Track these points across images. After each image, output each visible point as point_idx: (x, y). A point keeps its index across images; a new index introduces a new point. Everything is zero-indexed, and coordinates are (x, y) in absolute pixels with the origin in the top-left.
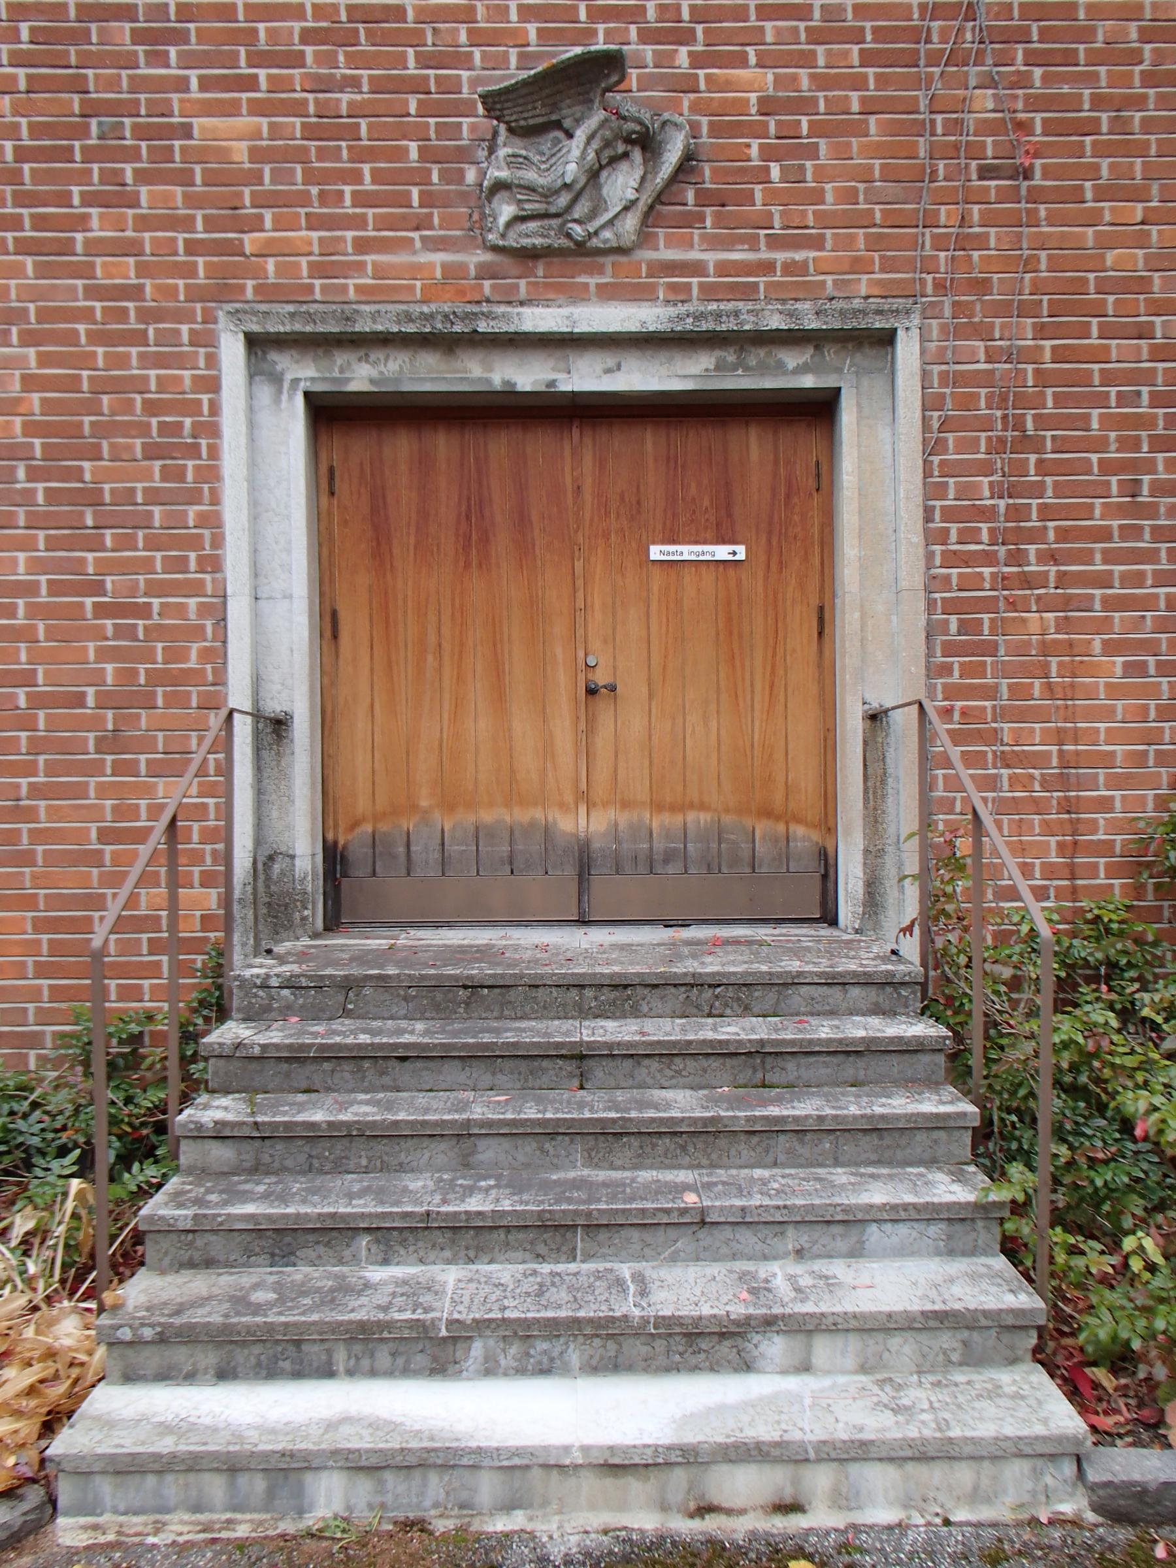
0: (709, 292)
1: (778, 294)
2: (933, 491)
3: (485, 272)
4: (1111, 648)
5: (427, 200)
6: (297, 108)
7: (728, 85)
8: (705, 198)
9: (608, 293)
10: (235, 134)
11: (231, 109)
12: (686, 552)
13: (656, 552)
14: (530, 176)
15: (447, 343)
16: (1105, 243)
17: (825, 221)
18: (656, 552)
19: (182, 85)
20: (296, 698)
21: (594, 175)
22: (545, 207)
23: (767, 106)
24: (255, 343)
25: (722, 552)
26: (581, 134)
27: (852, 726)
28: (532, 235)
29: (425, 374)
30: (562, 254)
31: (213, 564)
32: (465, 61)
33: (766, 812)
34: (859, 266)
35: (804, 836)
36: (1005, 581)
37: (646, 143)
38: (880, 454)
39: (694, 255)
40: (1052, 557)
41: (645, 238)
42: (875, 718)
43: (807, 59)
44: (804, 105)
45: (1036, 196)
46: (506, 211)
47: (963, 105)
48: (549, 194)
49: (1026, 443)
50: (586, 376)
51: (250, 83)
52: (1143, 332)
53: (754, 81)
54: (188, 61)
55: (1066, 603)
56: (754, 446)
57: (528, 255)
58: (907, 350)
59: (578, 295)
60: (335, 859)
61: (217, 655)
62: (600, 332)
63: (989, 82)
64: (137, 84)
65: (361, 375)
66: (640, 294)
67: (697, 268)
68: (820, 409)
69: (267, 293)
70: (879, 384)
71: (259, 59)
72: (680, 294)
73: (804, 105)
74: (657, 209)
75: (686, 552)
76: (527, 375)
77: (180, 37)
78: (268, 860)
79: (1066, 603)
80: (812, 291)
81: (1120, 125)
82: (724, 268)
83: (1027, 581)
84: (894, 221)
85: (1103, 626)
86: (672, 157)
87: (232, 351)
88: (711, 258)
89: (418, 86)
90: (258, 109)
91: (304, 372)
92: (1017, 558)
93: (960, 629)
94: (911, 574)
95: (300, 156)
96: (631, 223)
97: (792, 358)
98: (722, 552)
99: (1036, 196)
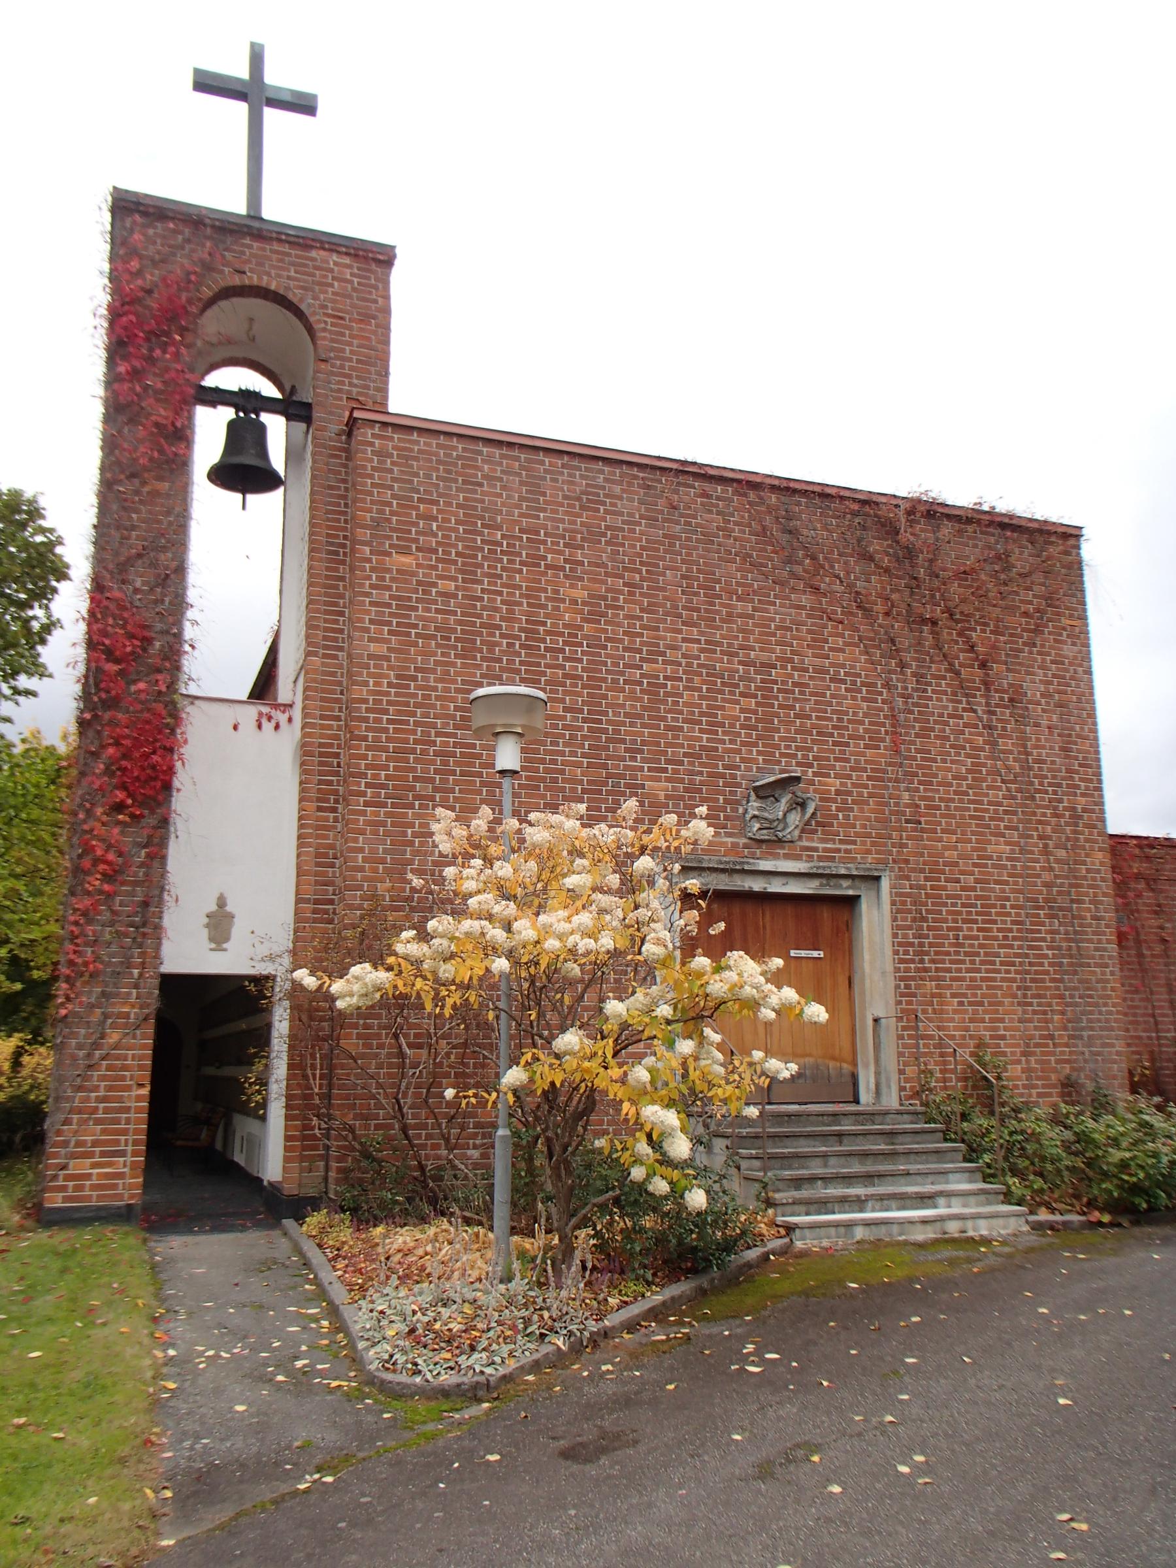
0: (820, 859)
1: (843, 860)
2: (895, 936)
3: (746, 846)
4: (953, 996)
5: (726, 818)
6: (682, 781)
7: (825, 784)
8: (818, 824)
9: (787, 857)
11: (659, 780)
12: (803, 953)
14: (766, 815)
15: (731, 872)
16: (945, 848)
17: (857, 835)
18: (793, 953)
19: (641, 769)
22: (769, 825)
23: (838, 793)
25: (815, 954)
26: (784, 801)
27: (870, 1023)
28: (764, 835)
30: (774, 844)
32: (738, 768)
33: (834, 1058)
34: (868, 852)
35: (846, 1067)
36: (918, 970)
37: (803, 805)
38: (875, 922)
39: (814, 845)
40: (933, 961)
41: (800, 838)
42: (876, 1020)
43: (849, 777)
44: (849, 793)
45: (923, 830)
46: (757, 826)
47: (899, 797)
48: (772, 821)
49: (925, 920)
50: (776, 887)
51: (665, 770)
52: (958, 881)
53: (834, 784)
54: (644, 760)
55: (938, 979)
56: (825, 913)
58: (885, 884)
59: (776, 857)
62: (784, 872)
63: (907, 790)
64: (626, 768)
66: (797, 858)
67: (816, 849)
68: (851, 902)
70: (873, 893)
71: (668, 762)
73: (849, 793)
75: (803, 953)
76: (757, 885)
77: (641, 752)
79: (938, 979)
81: (948, 808)
82: (825, 850)
83: (926, 970)
84: (879, 836)
85: (950, 987)
86: (810, 810)
88: (821, 846)
89: (723, 776)
90: (668, 780)
92: (922, 961)
94: (889, 968)
95: (682, 798)
96: (797, 833)
97: (845, 883)
98: (815, 954)
99: (923, 830)
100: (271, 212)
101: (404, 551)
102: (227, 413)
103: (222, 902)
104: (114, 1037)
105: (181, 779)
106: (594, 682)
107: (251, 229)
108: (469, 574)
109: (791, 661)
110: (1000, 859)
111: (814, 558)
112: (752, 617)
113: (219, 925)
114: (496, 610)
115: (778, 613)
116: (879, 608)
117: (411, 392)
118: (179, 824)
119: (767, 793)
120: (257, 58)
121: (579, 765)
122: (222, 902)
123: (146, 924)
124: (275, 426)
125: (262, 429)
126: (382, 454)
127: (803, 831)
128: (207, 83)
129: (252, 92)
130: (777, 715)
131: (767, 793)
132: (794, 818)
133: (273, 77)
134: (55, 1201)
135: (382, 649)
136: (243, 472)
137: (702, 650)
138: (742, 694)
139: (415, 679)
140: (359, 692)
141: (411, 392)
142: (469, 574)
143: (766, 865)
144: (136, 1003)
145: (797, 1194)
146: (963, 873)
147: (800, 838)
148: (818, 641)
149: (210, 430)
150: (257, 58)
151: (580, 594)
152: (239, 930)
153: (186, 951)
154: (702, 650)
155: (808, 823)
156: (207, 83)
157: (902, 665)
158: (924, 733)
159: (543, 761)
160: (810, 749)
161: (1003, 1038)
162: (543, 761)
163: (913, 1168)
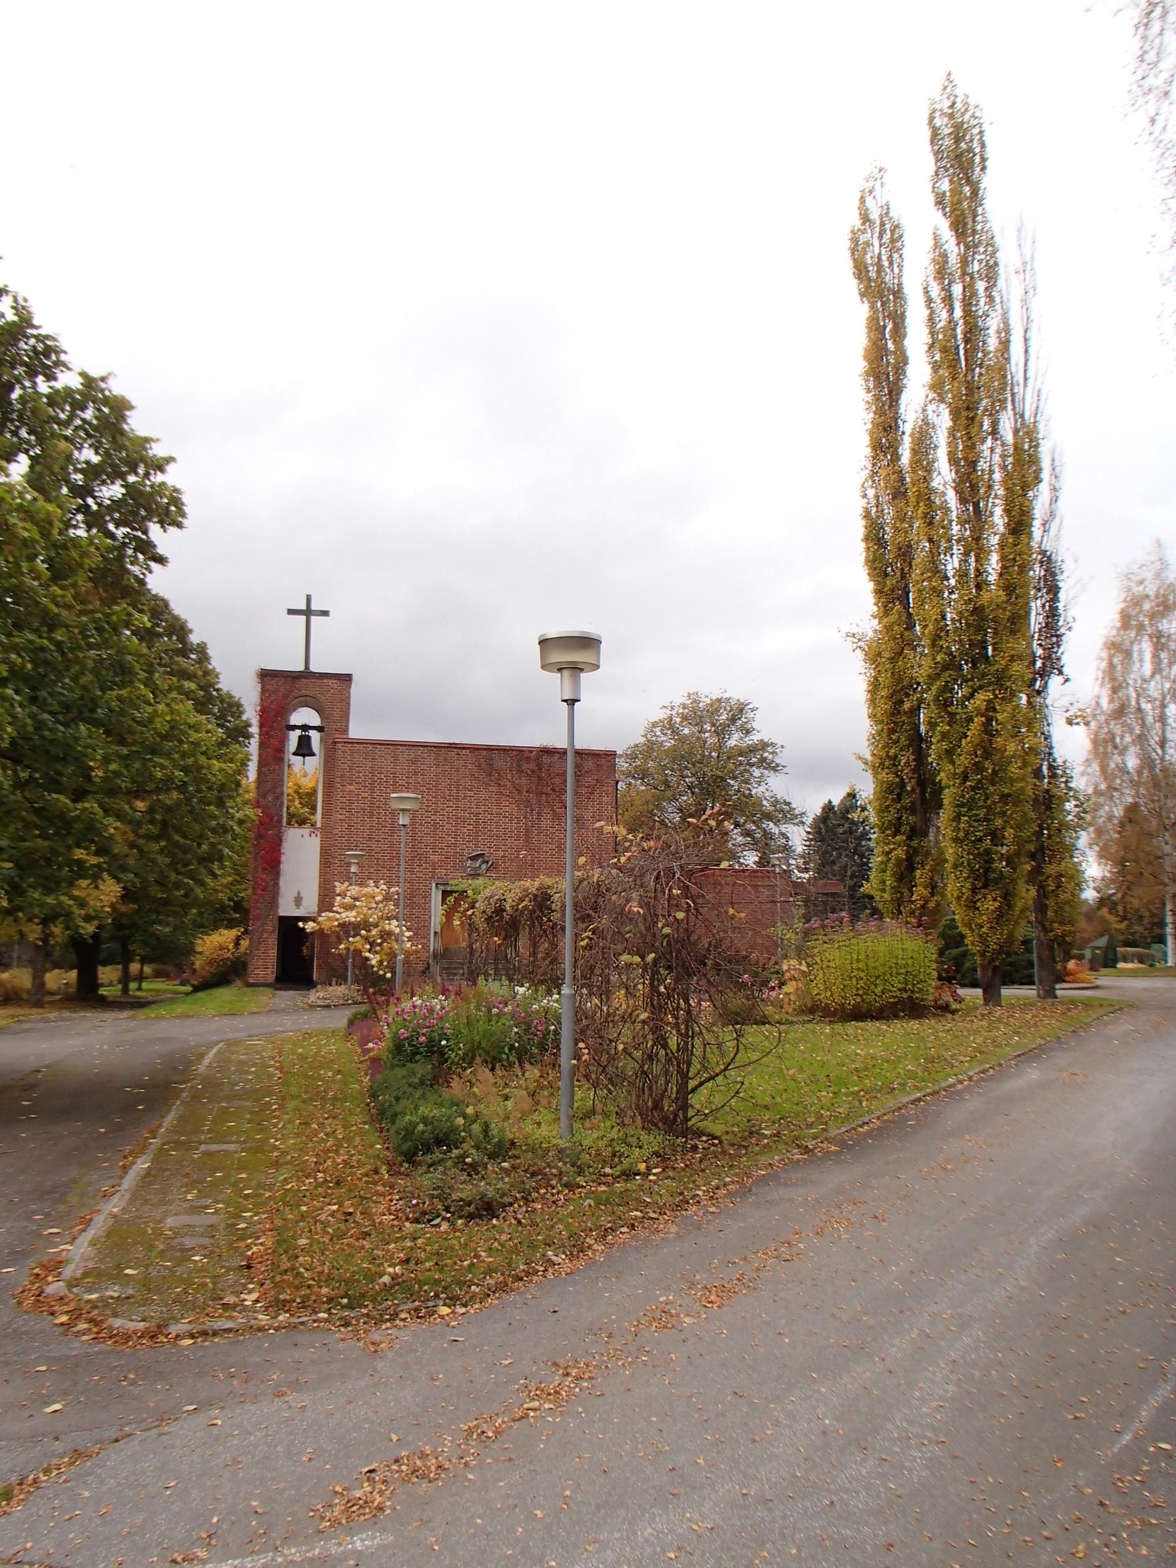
10: (436, 858)
20: (439, 930)
22: (475, 869)
87: (434, 885)
91: (442, 888)
100: (313, 668)
101: (351, 784)
102: (298, 732)
103: (299, 893)
104: (265, 935)
105: (283, 858)
107: (307, 674)
111: (499, 774)
113: (298, 901)
115: (483, 795)
116: (524, 789)
117: (356, 731)
118: (282, 872)
119: (474, 858)
120: (309, 599)
122: (299, 893)
123: (274, 903)
124: (315, 736)
125: (309, 738)
128: (291, 612)
129: (308, 613)
131: (474, 858)
132: (484, 866)
133: (314, 607)
134: (251, 981)
136: (304, 749)
140: (336, 831)
141: (356, 731)
144: (271, 926)
148: (499, 804)
149: (294, 736)
150: (309, 599)
152: (304, 902)
153: (286, 909)
156: (291, 612)
157: (532, 810)
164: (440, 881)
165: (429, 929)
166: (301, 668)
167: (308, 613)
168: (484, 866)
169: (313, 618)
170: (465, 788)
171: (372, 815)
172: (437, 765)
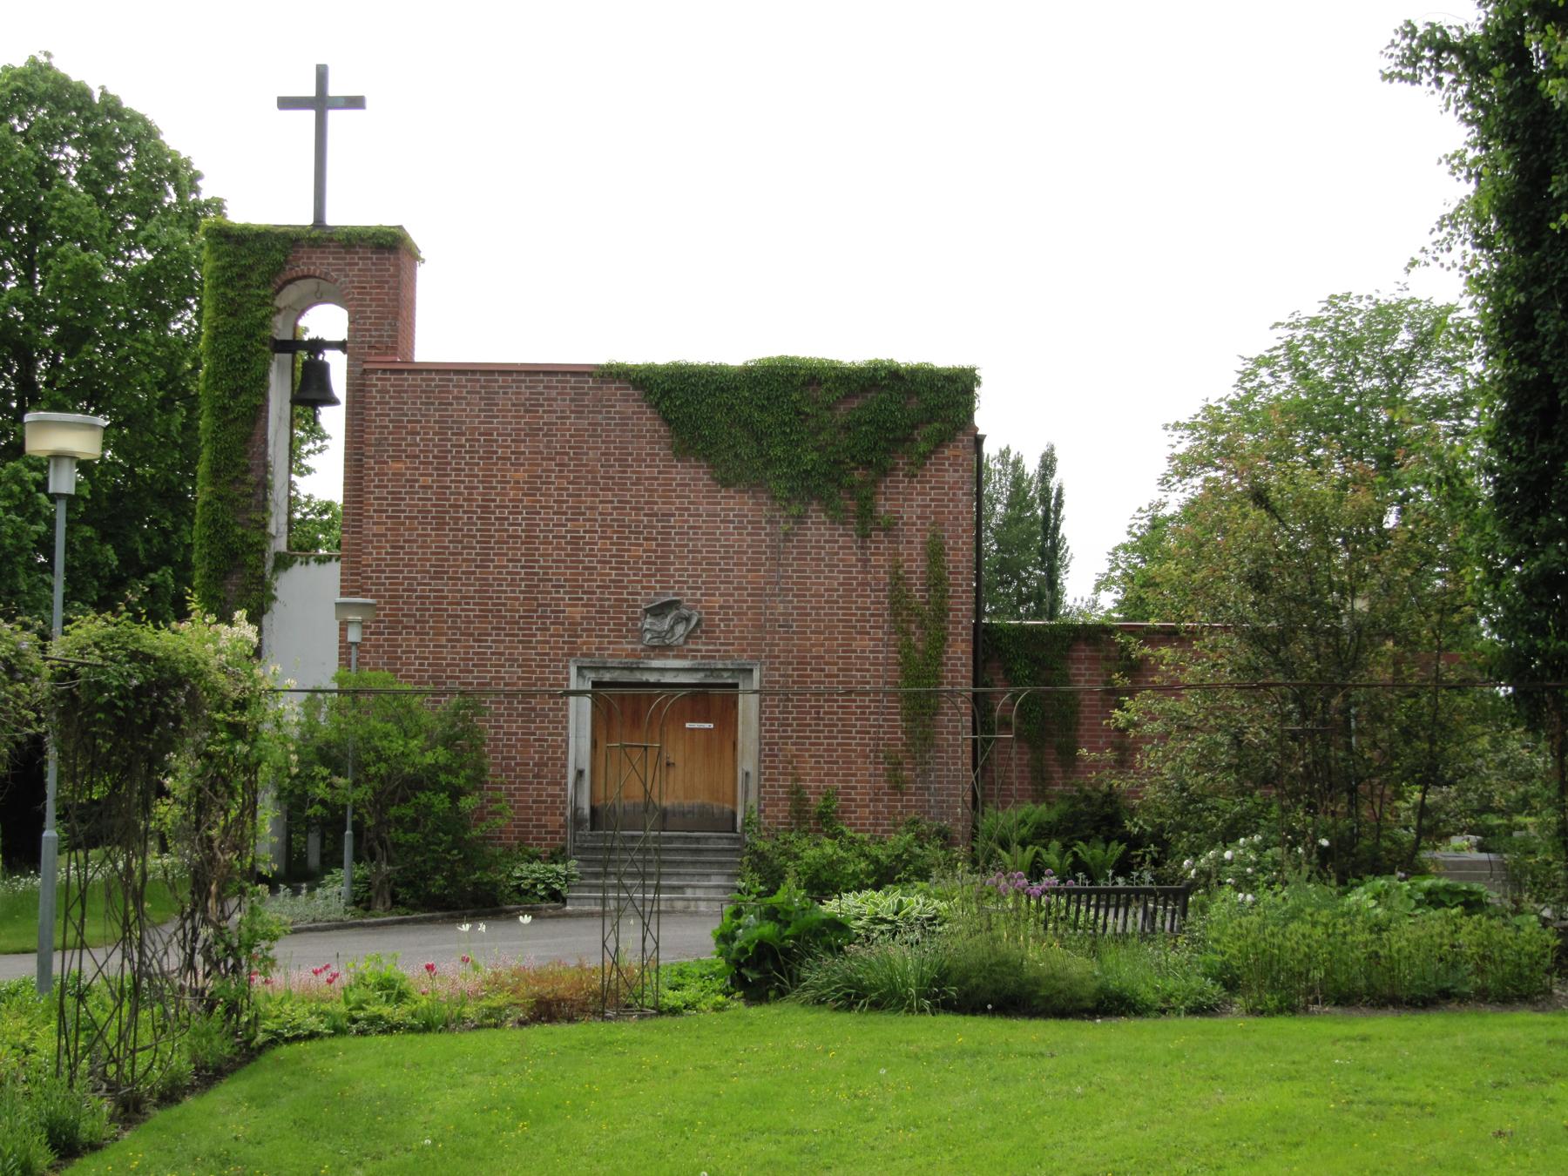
0: (703, 657)
1: (721, 658)
2: (762, 712)
9: (675, 657)
10: (578, 612)
12: (696, 725)
13: (688, 725)
15: (631, 669)
18: (688, 725)
20: (586, 767)
21: (672, 628)
22: (659, 635)
23: (721, 607)
24: (580, 669)
25: (706, 726)
28: (655, 642)
29: (625, 677)
30: (663, 649)
31: (565, 728)
34: (744, 651)
35: (728, 807)
37: (688, 620)
41: (686, 642)
49: (788, 700)
50: (668, 678)
53: (718, 601)
57: (654, 648)
58: (756, 674)
59: (667, 657)
60: (593, 810)
61: (566, 753)
62: (672, 669)
65: (607, 677)
66: (685, 657)
69: (583, 655)
72: (695, 657)
74: (689, 636)
75: (696, 725)
76: (652, 678)
78: (576, 809)
80: (731, 657)
86: (694, 622)
87: (573, 671)
89: (627, 600)
93: (768, 751)
96: (682, 640)
97: (726, 675)
98: (706, 726)
101: (397, 459)
106: (530, 539)
108: (441, 470)
109: (688, 509)
110: (863, 652)
112: (656, 479)
114: (461, 494)
119: (659, 611)
121: (517, 599)
126: (383, 391)
127: (688, 637)
130: (673, 552)
131: (659, 611)
132: (680, 629)
135: (381, 529)
137: (614, 508)
138: (645, 539)
139: (402, 548)
142: (441, 470)
143: (656, 663)
145: (594, 882)
146: (826, 664)
147: (686, 642)
151: (522, 475)
154: (614, 508)
155: (693, 630)
158: (801, 557)
159: (491, 598)
160: (700, 576)
161: (854, 788)
162: (491, 598)
163: (682, 871)
164: (586, 662)
165: (565, 766)
166: (307, 219)
167: (321, 103)
168: (680, 629)
169: (310, 115)
170: (639, 460)
171: (441, 525)
172: (579, 413)
